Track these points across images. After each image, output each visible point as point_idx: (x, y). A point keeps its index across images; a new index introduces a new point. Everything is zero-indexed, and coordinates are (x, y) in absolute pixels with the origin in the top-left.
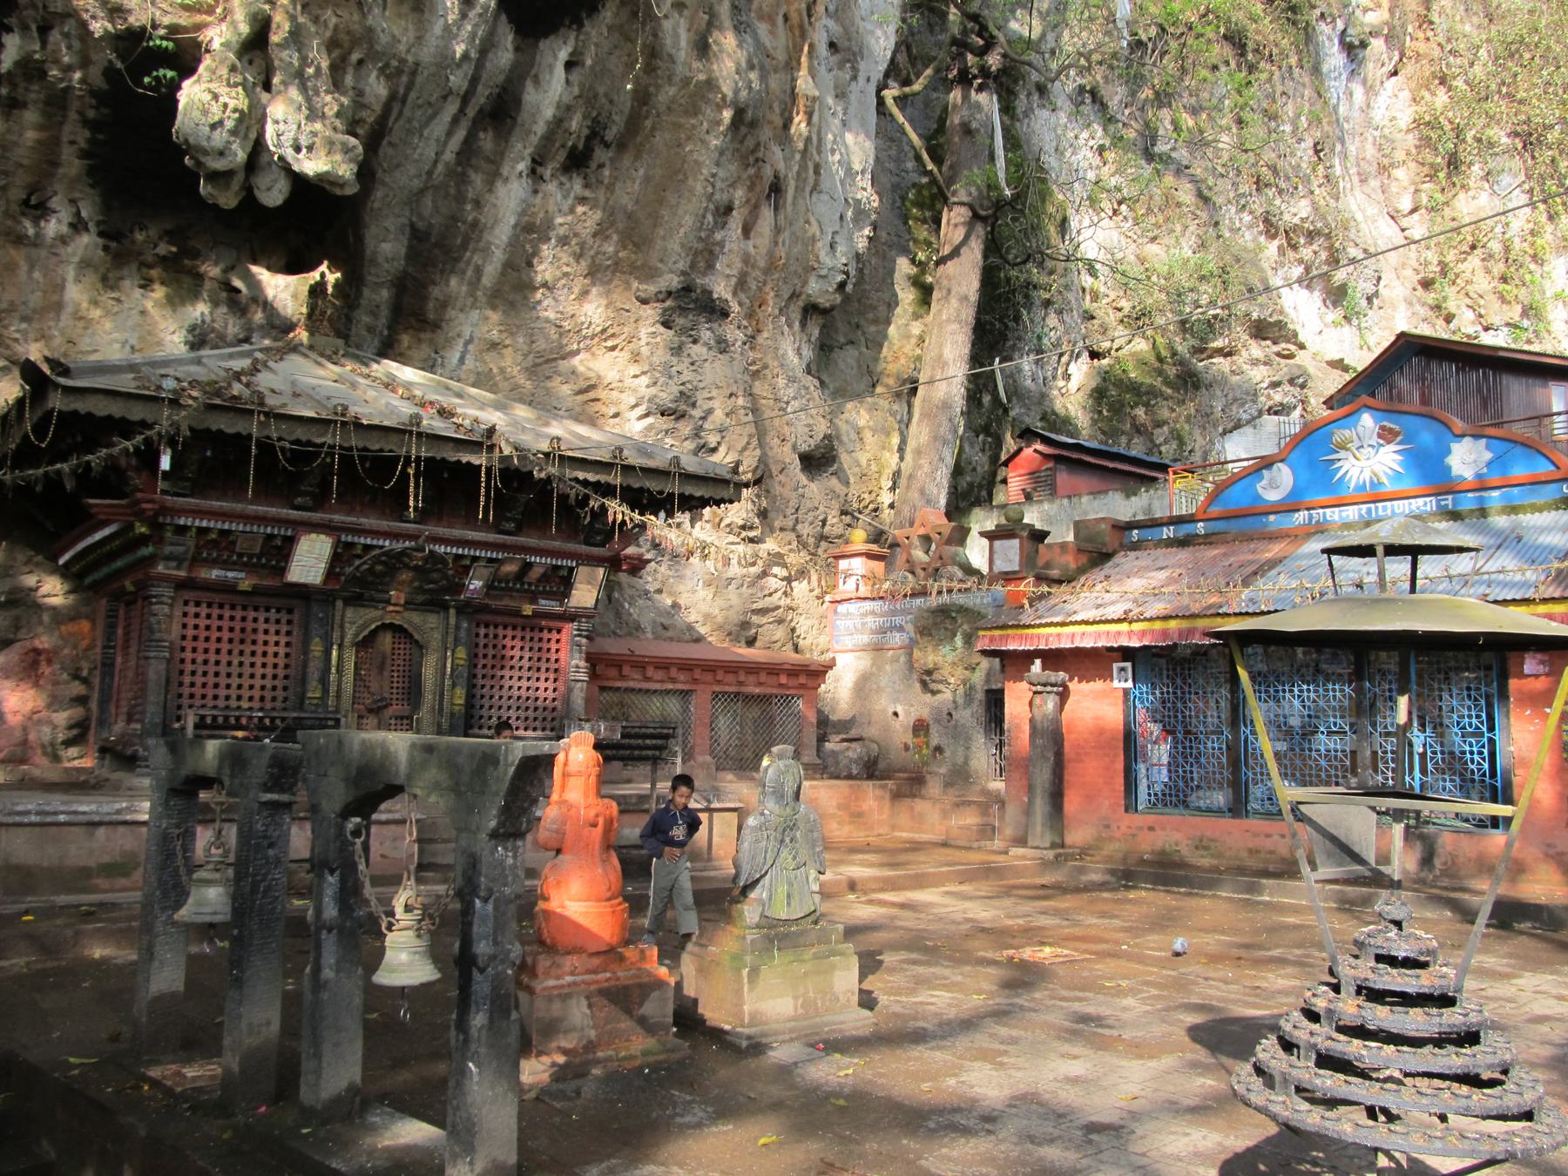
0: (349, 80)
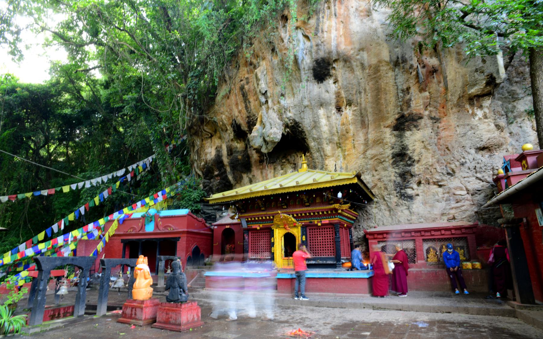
0: (284, 116)
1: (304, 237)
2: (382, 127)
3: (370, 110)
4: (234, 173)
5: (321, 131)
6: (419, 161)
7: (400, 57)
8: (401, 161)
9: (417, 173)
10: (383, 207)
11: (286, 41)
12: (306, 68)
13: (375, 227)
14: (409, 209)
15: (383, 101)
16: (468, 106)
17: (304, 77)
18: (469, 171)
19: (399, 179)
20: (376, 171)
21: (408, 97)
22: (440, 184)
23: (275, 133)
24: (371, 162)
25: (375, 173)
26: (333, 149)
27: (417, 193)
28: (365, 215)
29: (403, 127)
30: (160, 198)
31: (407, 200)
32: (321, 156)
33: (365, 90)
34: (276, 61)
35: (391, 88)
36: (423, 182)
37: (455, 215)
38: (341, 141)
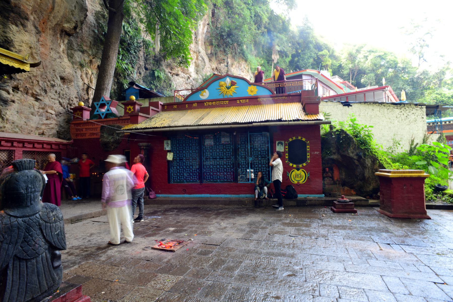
16: (59, 36)
18: (56, 94)
22: (38, 97)
37: (45, 131)
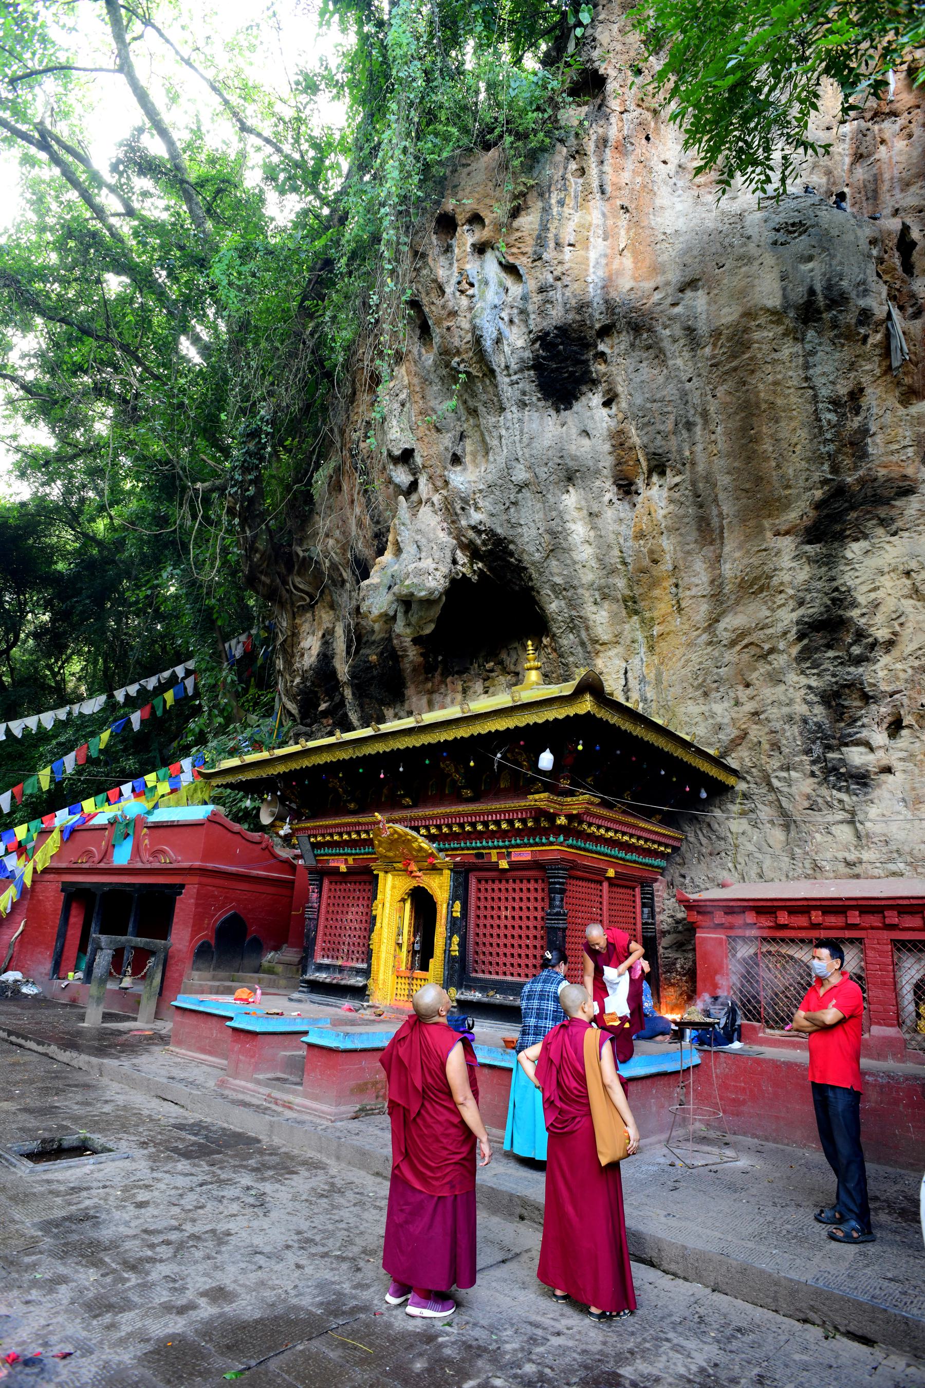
0: (464, 523)
1: (458, 906)
2: (769, 534)
3: (724, 480)
4: (361, 706)
5: (575, 563)
6: (890, 644)
7: (818, 288)
8: (829, 647)
9: (884, 687)
10: (765, 813)
11: (449, 290)
12: (514, 367)
13: (723, 886)
14: (852, 822)
15: (767, 446)
17: (508, 392)
19: (819, 713)
20: (748, 685)
21: (855, 422)
23: (419, 573)
24: (730, 656)
25: (743, 694)
26: (614, 616)
27: (884, 762)
28: (704, 841)
29: (838, 527)
30: (186, 778)
31: (847, 790)
32: (583, 644)
33: (705, 414)
34: (429, 358)
35: (793, 399)
36: (908, 720)
38: (638, 591)
